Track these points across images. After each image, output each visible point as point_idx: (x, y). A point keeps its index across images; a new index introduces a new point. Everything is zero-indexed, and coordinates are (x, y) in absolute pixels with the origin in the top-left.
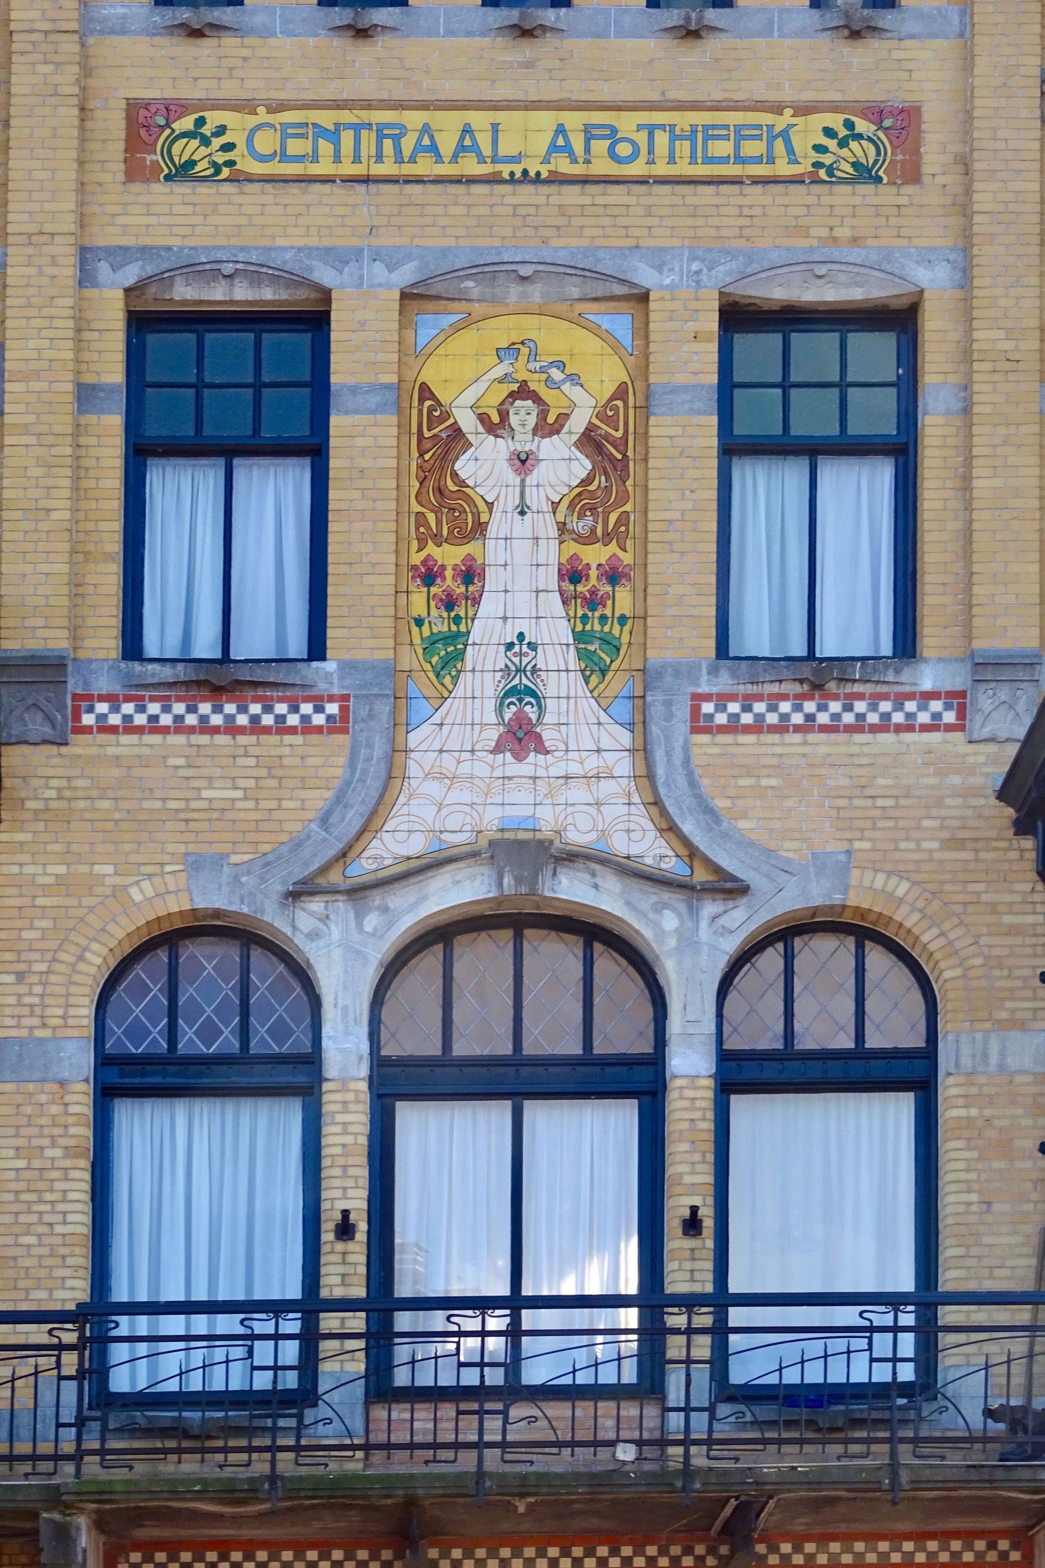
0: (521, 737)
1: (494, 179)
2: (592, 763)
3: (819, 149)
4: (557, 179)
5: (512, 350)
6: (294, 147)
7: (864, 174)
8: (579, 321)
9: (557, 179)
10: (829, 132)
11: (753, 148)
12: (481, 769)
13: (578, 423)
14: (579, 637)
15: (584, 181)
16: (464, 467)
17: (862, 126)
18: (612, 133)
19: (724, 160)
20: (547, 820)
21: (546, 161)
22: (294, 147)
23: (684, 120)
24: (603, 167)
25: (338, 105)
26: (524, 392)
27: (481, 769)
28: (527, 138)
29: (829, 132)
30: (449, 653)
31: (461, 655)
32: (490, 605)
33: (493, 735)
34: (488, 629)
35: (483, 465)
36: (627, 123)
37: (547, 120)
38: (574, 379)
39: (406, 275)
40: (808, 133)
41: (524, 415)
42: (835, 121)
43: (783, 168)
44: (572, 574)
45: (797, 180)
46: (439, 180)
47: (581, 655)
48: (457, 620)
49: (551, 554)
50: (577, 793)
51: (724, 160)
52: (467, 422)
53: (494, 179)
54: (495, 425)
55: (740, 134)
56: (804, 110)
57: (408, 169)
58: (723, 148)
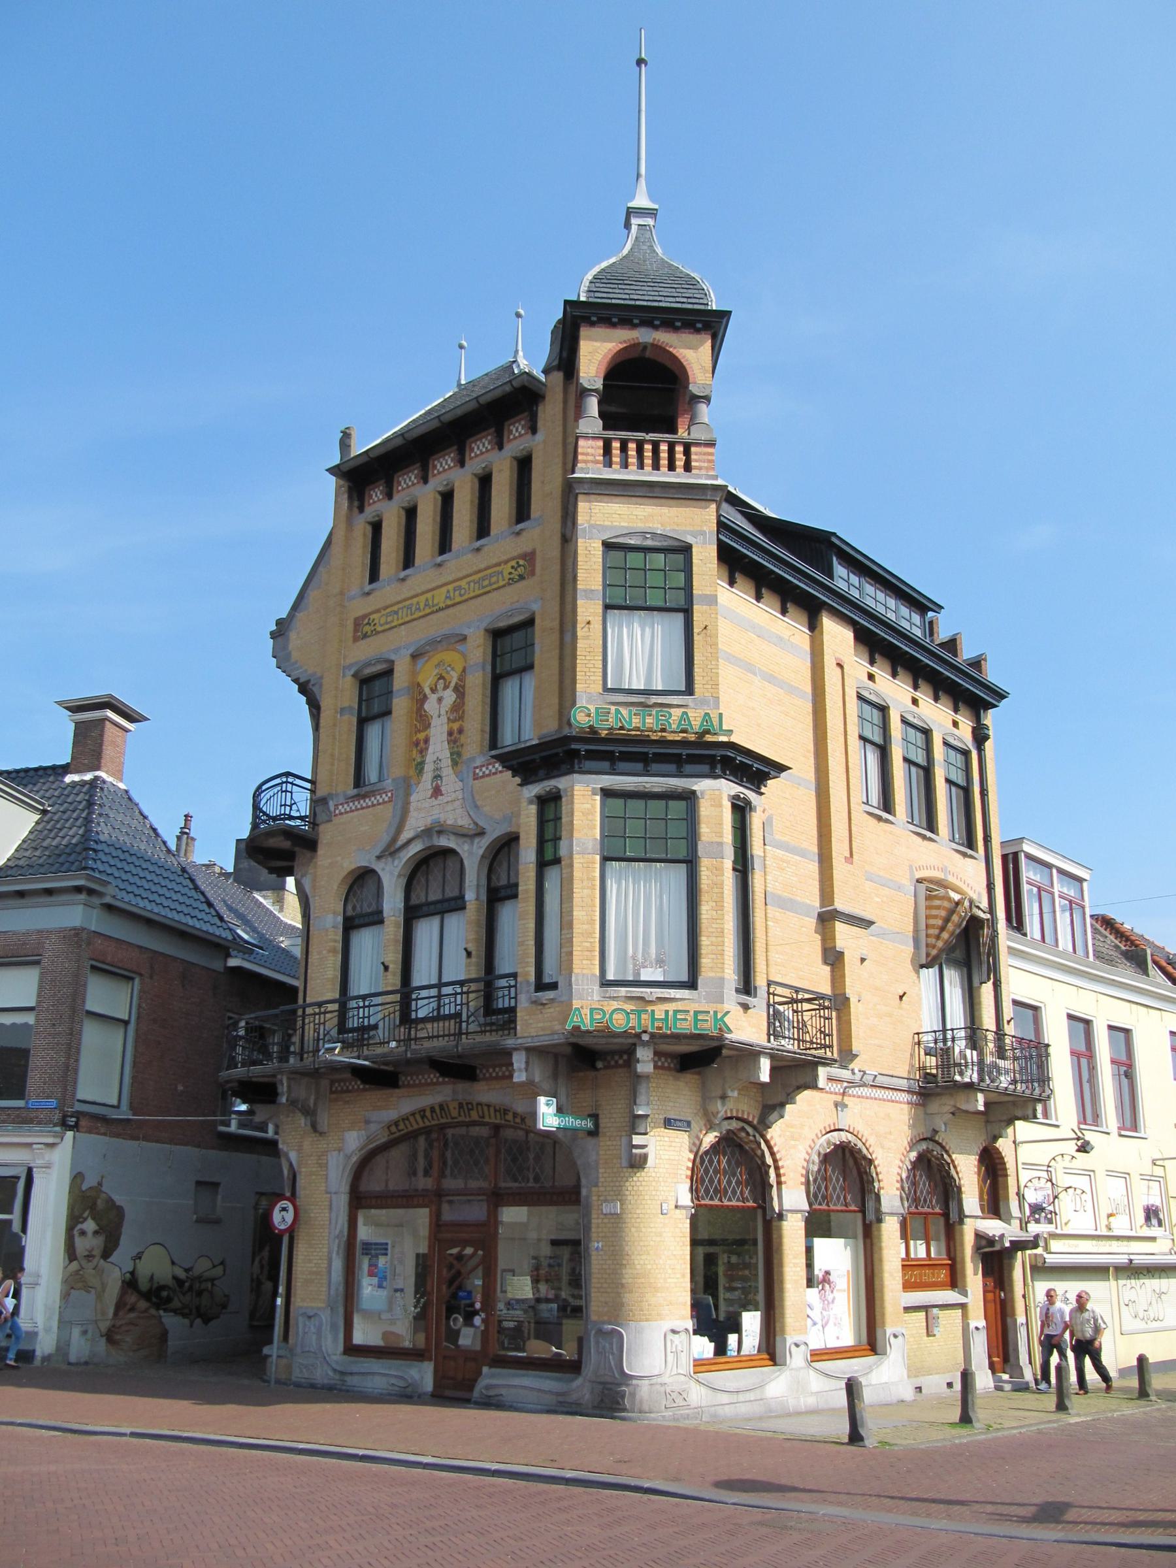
0: (437, 792)
1: (432, 613)
2: (454, 796)
3: (510, 573)
4: (448, 607)
7: (522, 577)
8: (454, 650)
9: (448, 607)
11: (494, 579)
12: (427, 805)
13: (453, 685)
14: (452, 754)
16: (426, 706)
17: (521, 562)
18: (460, 588)
20: (442, 817)
22: (389, 619)
23: (476, 577)
24: (458, 599)
25: (399, 603)
26: (441, 677)
27: (426, 804)
30: (420, 767)
31: (422, 769)
32: (430, 750)
34: (430, 758)
35: (430, 706)
36: (463, 583)
37: (444, 590)
38: (453, 669)
40: (507, 569)
42: (513, 563)
43: (501, 583)
44: (450, 733)
45: (504, 586)
46: (423, 616)
47: (452, 760)
49: (445, 728)
50: (450, 807)
52: (427, 691)
53: (432, 613)
54: (433, 691)
55: (491, 576)
56: (506, 562)
58: (486, 583)
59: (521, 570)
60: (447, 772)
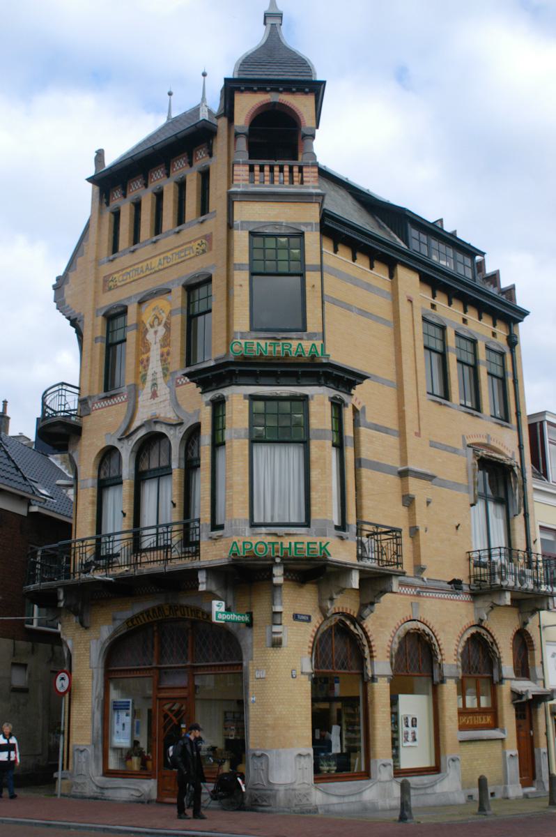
0: (154, 395)
3: (197, 249)
5: (154, 309)
6: (125, 278)
10: (199, 244)
13: (163, 322)
15: (165, 269)
18: (167, 258)
19: (183, 257)
21: (158, 266)
22: (125, 278)
28: (155, 263)
29: (199, 244)
31: (146, 379)
33: (150, 395)
34: (150, 372)
38: (163, 312)
39: (138, 299)
40: (195, 245)
41: (156, 323)
48: (145, 371)
51: (183, 257)
54: (152, 326)
57: (140, 276)
59: (203, 246)
60: (160, 381)
